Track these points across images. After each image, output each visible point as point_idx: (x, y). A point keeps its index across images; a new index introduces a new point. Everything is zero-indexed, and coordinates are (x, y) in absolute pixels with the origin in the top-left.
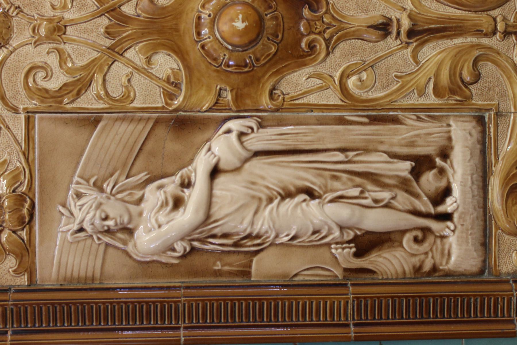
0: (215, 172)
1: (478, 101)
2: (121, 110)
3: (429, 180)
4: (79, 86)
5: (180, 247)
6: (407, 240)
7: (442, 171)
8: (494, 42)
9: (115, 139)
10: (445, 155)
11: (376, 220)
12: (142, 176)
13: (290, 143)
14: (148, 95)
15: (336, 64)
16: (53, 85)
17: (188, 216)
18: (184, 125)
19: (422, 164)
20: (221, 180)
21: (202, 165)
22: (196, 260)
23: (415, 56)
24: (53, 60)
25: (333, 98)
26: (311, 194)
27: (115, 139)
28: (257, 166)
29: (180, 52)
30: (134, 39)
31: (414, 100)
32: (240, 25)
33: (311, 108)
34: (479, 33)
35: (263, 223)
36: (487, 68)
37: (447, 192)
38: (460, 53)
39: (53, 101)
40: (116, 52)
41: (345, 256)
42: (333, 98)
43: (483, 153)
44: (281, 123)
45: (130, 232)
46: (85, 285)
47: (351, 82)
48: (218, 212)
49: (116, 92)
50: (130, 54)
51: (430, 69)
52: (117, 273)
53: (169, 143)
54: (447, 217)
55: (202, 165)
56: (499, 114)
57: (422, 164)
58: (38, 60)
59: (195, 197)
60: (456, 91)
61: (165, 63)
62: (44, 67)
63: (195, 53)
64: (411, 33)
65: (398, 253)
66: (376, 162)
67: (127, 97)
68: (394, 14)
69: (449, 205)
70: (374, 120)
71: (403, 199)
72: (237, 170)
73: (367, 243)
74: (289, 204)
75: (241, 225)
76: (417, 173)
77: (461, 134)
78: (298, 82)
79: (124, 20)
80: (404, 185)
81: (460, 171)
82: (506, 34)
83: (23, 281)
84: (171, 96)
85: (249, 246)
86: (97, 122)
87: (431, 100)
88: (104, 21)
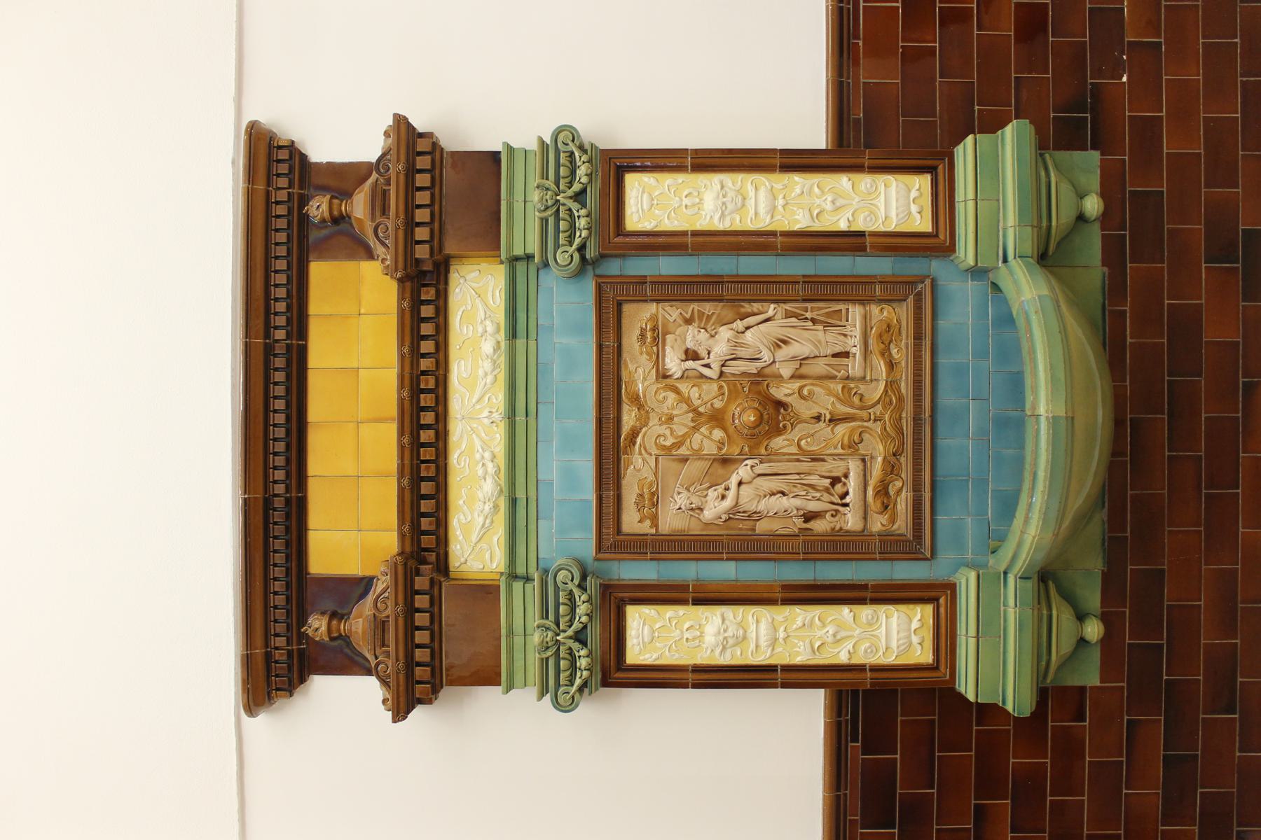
0: (740, 483)
1: (862, 452)
2: (698, 455)
3: (838, 487)
4: (678, 445)
5: (724, 517)
6: (828, 515)
7: (845, 484)
8: (869, 424)
9: (695, 468)
10: (846, 476)
11: (813, 506)
12: (707, 485)
13: (775, 471)
14: (710, 448)
15: (795, 434)
16: (668, 443)
17: (728, 503)
18: (726, 462)
19: (835, 481)
20: (743, 487)
21: (734, 480)
22: (731, 523)
23: (832, 430)
24: (668, 432)
25: (794, 450)
26: (784, 494)
27: (695, 468)
28: (759, 481)
29: (724, 429)
30: (703, 424)
31: (832, 451)
32: (752, 419)
33: (785, 454)
34: (862, 420)
35: (762, 506)
36: (866, 436)
37: (847, 493)
38: (853, 430)
39: (667, 450)
40: (696, 429)
41: (799, 522)
42: (794, 450)
43: (865, 475)
44: (770, 461)
45: (701, 510)
46: (682, 534)
47: (803, 443)
48: (741, 501)
49: (696, 447)
50: (703, 430)
51: (839, 436)
52: (696, 529)
53: (720, 471)
54: (846, 505)
55: (734, 480)
56: (872, 458)
57: (835, 481)
58: (661, 432)
59: (731, 495)
60: (852, 446)
61: (718, 434)
62: (664, 436)
63: (731, 430)
64: (830, 421)
65: (824, 521)
66: (814, 480)
67: (700, 449)
68: (823, 411)
69: (847, 500)
70: (814, 460)
71: (826, 497)
72: (750, 482)
73: (809, 517)
74: (774, 498)
75: (752, 507)
76: (833, 484)
77: (854, 467)
78: (778, 443)
79: (700, 414)
80: (827, 490)
81: (853, 484)
82: (875, 420)
83: (653, 531)
84: (720, 449)
85: (755, 517)
86: (687, 460)
87: (840, 451)
88: (691, 415)
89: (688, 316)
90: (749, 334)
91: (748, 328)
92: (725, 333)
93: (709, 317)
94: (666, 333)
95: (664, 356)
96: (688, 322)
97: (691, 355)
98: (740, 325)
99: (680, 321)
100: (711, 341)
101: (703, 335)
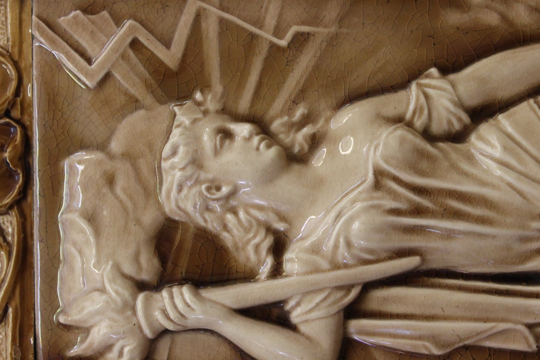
89: (170, 57)
90: (488, 144)
91: (482, 112)
92: (359, 142)
93: (279, 60)
94: (63, 144)
95: (53, 261)
96: (174, 84)
97: (185, 256)
98: (439, 96)
99: (130, 80)
100: (289, 186)
101: (244, 156)
